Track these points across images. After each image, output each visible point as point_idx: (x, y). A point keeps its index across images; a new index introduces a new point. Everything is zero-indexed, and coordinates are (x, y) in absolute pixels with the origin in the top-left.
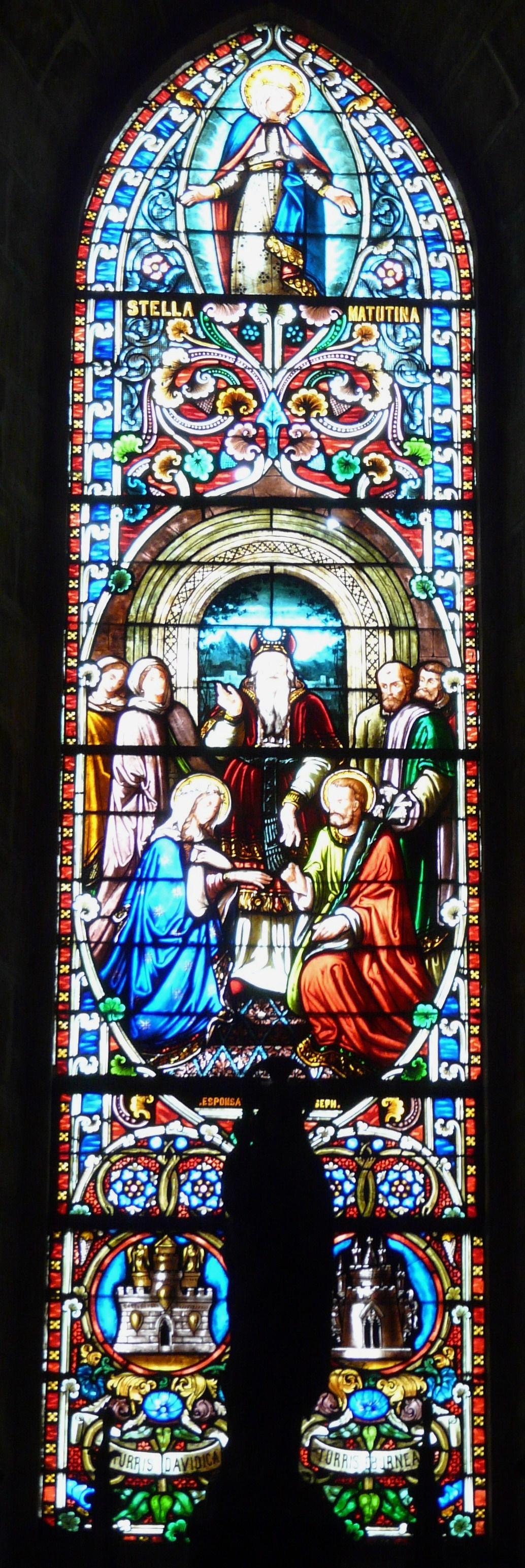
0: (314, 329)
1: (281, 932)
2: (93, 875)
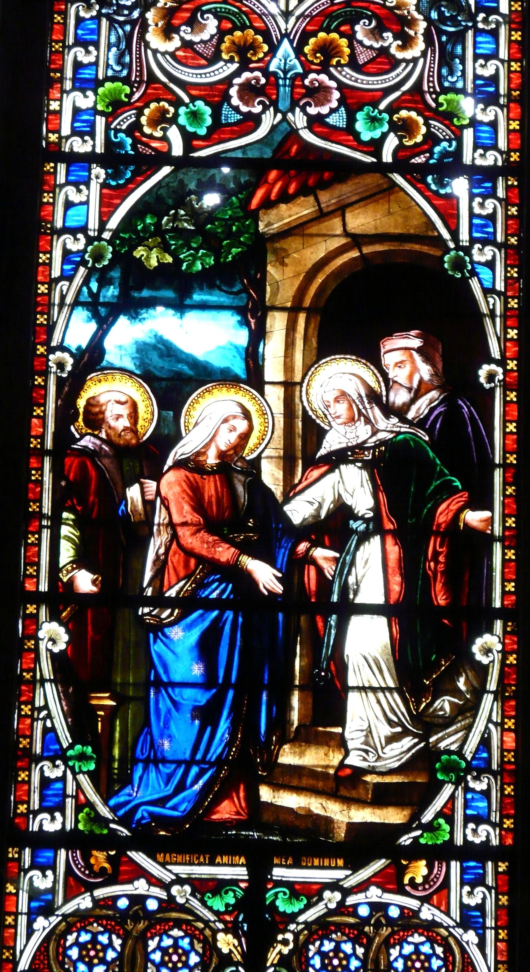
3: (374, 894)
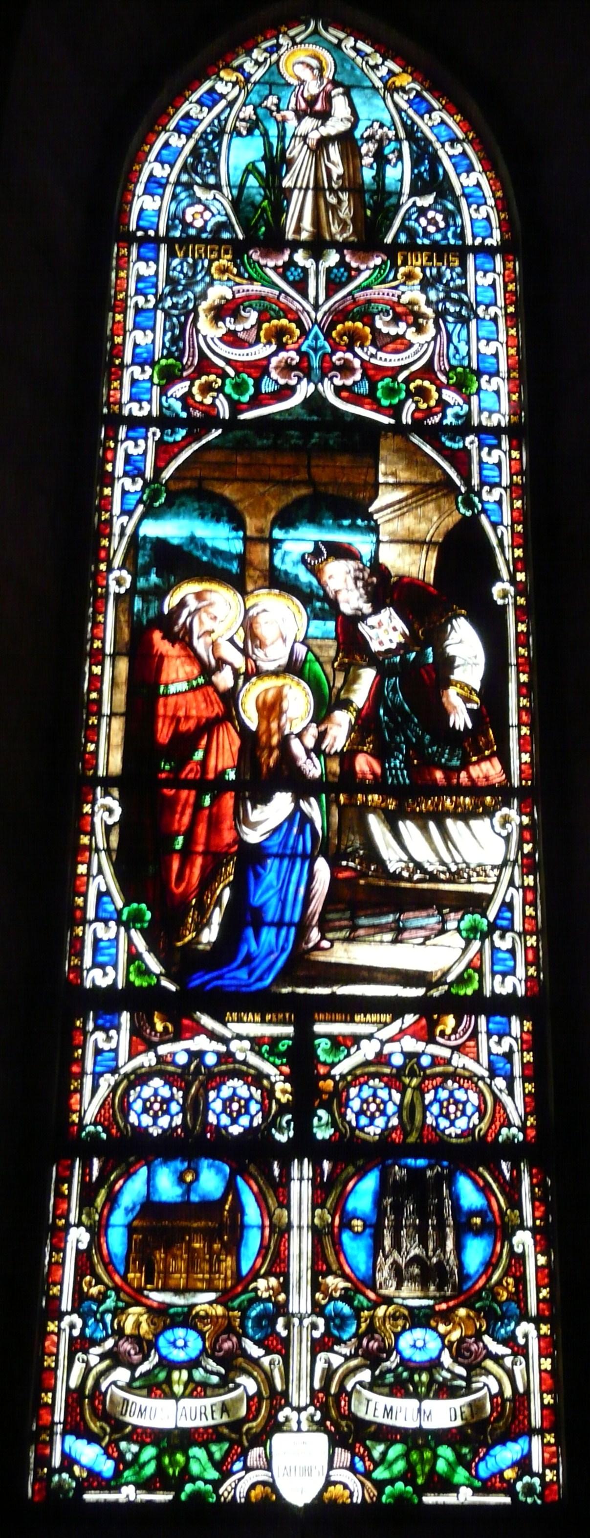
0: (359, 271)
3: (410, 1044)
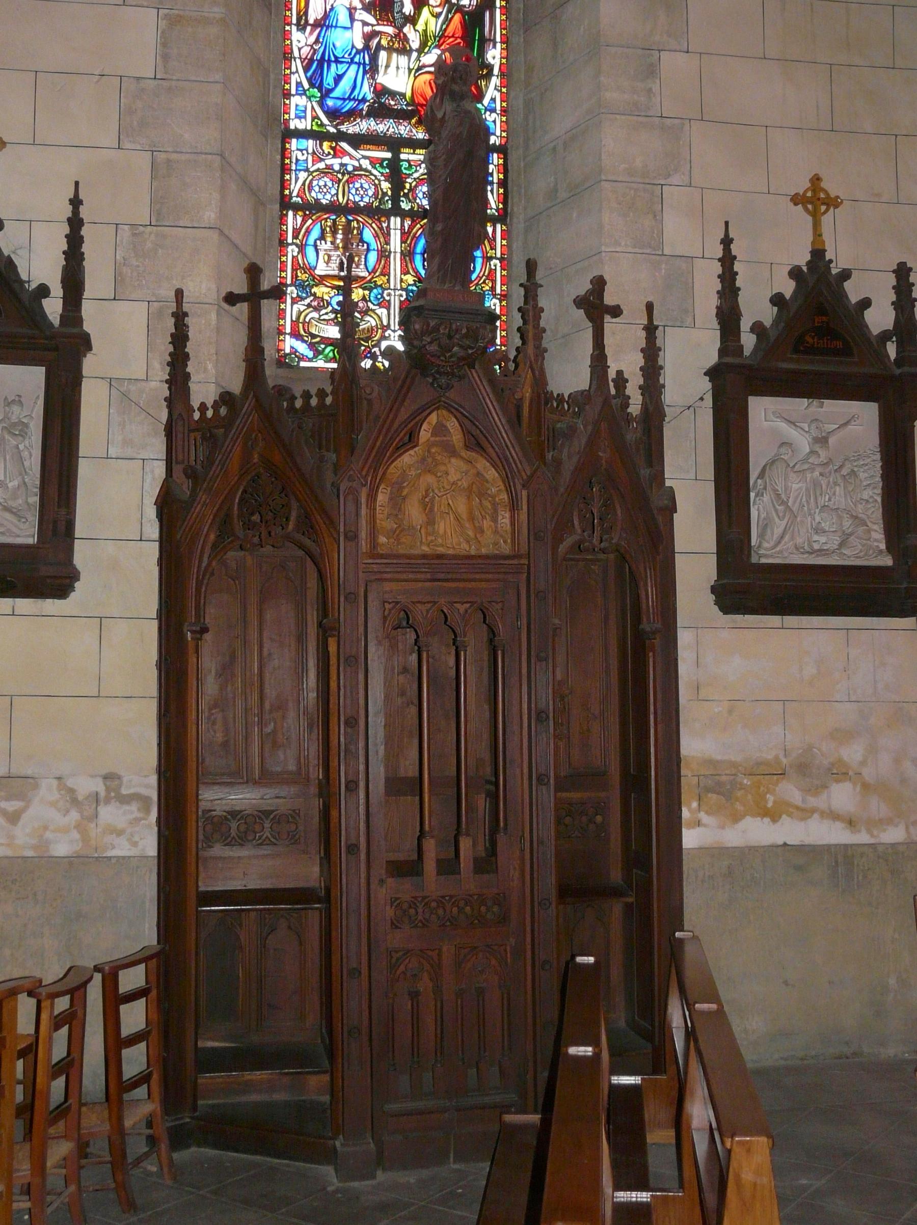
1: (403, 60)
2: (303, 22)
